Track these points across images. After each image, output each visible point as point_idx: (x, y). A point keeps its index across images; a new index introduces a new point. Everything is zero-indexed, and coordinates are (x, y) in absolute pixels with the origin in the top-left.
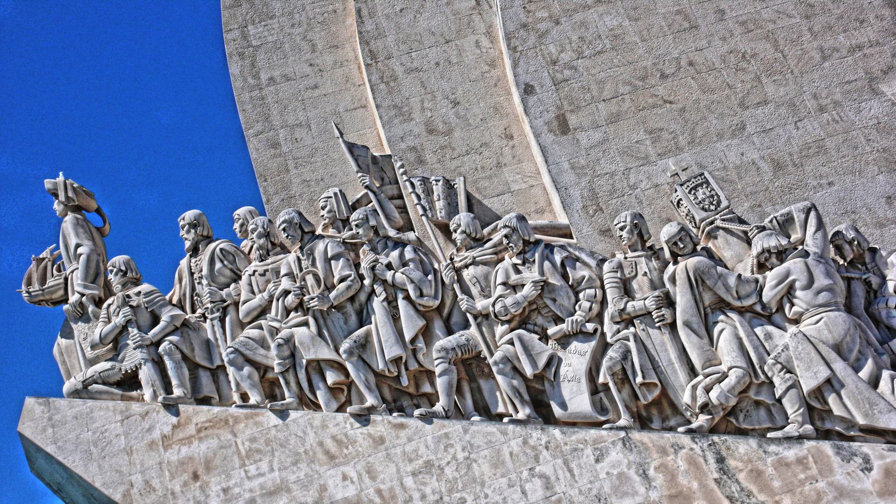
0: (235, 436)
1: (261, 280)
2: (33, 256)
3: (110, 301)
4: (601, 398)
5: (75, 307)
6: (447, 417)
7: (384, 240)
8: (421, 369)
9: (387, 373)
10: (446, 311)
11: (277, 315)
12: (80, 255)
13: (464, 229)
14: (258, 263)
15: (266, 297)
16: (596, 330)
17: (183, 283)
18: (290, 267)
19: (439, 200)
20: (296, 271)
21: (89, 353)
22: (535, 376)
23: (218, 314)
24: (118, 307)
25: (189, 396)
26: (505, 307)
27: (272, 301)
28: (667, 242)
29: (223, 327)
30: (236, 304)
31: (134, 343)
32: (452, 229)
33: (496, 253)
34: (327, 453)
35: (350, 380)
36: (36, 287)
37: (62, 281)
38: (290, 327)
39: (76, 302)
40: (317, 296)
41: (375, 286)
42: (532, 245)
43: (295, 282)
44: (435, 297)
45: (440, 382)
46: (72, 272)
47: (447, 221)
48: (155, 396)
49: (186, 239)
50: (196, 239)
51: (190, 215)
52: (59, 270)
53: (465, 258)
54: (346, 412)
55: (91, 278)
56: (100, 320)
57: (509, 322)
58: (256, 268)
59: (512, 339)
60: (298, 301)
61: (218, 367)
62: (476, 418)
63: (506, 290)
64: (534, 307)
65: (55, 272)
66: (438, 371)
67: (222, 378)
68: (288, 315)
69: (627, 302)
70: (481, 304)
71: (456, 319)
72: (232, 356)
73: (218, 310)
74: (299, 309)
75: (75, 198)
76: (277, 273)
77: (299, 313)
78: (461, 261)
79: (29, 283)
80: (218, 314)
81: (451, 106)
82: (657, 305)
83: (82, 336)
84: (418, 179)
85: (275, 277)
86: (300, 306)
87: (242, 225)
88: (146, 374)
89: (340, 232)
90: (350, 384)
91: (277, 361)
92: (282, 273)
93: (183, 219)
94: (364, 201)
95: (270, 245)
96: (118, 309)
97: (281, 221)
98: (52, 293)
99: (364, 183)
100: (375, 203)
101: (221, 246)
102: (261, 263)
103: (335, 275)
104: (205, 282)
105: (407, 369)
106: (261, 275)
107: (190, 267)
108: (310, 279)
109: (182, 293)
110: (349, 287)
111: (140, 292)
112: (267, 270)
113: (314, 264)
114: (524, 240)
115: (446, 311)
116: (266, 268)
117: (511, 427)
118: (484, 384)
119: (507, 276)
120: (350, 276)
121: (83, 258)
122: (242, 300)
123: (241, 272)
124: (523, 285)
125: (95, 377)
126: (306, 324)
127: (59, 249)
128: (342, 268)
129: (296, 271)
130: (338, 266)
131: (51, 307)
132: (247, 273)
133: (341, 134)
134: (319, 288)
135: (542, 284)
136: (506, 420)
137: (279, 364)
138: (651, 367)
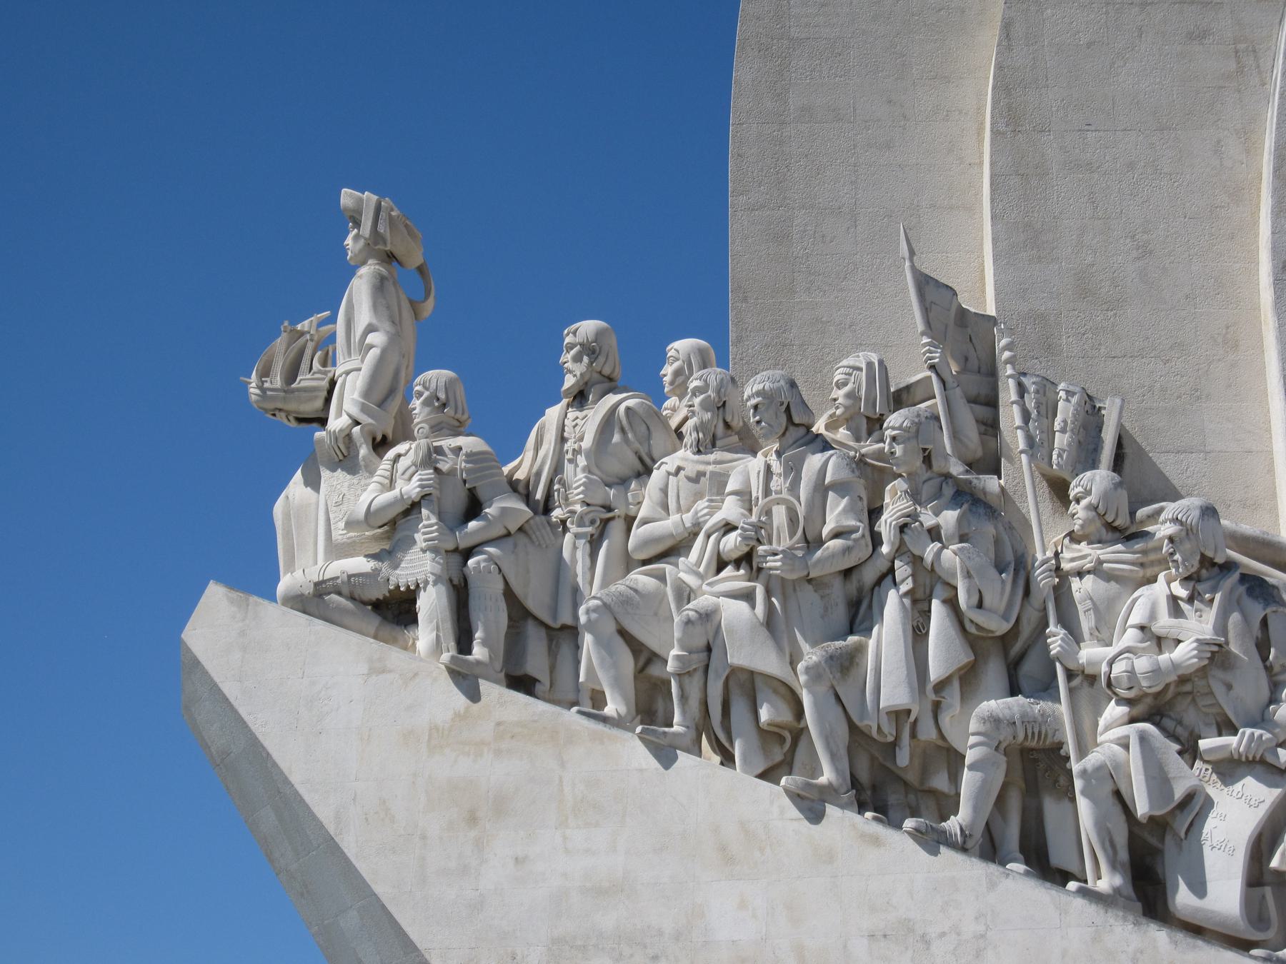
0: (563, 765)
1: (687, 487)
2: (286, 323)
3: (401, 448)
4: (1264, 897)
5: (336, 439)
6: (963, 849)
7: (939, 480)
8: (940, 743)
9: (874, 734)
10: (1016, 649)
12: (371, 347)
13: (1094, 502)
14: (689, 454)
15: (688, 524)
17: (541, 453)
18: (747, 482)
19: (1063, 431)
20: (757, 491)
21: (339, 533)
22: (1152, 819)
23: (589, 529)
24: (414, 464)
25: (498, 664)
26: (1132, 672)
27: (696, 535)
29: (593, 556)
30: (630, 521)
31: (426, 540)
32: (1072, 494)
33: (1142, 565)
34: (723, 848)
35: (802, 725)
36: (277, 381)
37: (325, 384)
38: (718, 595)
39: (341, 430)
40: (783, 552)
41: (897, 563)
42: (1216, 569)
43: (750, 511)
44: (1005, 617)
45: (969, 780)
46: (348, 373)
47: (1066, 476)
48: (437, 647)
49: (570, 371)
50: (586, 378)
51: (588, 327)
52: (324, 364)
54: (778, 783)
56: (375, 479)
59: (1128, 737)
60: (746, 549)
61: (564, 627)
62: (1018, 867)
63: (1142, 641)
64: (1188, 688)
65: (316, 365)
66: (970, 756)
67: (565, 650)
70: (1090, 653)
71: (1030, 667)
72: (594, 616)
73: (592, 522)
74: (744, 564)
75: (388, 236)
76: (719, 482)
77: (742, 572)
78: (1073, 560)
79: (265, 373)
80: (589, 529)
81: (1135, 254)
83: (335, 499)
84: (1035, 379)
85: (715, 490)
86: (746, 559)
87: (678, 373)
88: (431, 603)
89: (858, 440)
90: (800, 736)
91: (675, 652)
92: (729, 488)
93: (575, 333)
94: (919, 394)
95: (721, 425)
96: (413, 468)
97: (754, 391)
99: (930, 359)
100: (938, 400)
101: (631, 403)
102: (697, 457)
103: (827, 520)
104: (582, 461)
105: (913, 735)
106: (689, 479)
107: (564, 426)
108: (780, 514)
109: (534, 470)
110: (847, 550)
111: (460, 449)
112: (704, 474)
113: (794, 487)
114: (1203, 555)
115: (1016, 649)
116: (701, 468)
117: (1079, 902)
118: (1052, 809)
119: (1153, 615)
120: (856, 530)
121: (374, 354)
123: (654, 461)
124: (1179, 642)
125: (339, 581)
126: (748, 597)
127: (335, 322)
128: (845, 511)
129: (757, 491)
130: (838, 505)
131: (293, 424)
132: (664, 468)
133: (912, 253)
134: (791, 538)
135: (1215, 649)
136: (1072, 885)
137: (678, 657)
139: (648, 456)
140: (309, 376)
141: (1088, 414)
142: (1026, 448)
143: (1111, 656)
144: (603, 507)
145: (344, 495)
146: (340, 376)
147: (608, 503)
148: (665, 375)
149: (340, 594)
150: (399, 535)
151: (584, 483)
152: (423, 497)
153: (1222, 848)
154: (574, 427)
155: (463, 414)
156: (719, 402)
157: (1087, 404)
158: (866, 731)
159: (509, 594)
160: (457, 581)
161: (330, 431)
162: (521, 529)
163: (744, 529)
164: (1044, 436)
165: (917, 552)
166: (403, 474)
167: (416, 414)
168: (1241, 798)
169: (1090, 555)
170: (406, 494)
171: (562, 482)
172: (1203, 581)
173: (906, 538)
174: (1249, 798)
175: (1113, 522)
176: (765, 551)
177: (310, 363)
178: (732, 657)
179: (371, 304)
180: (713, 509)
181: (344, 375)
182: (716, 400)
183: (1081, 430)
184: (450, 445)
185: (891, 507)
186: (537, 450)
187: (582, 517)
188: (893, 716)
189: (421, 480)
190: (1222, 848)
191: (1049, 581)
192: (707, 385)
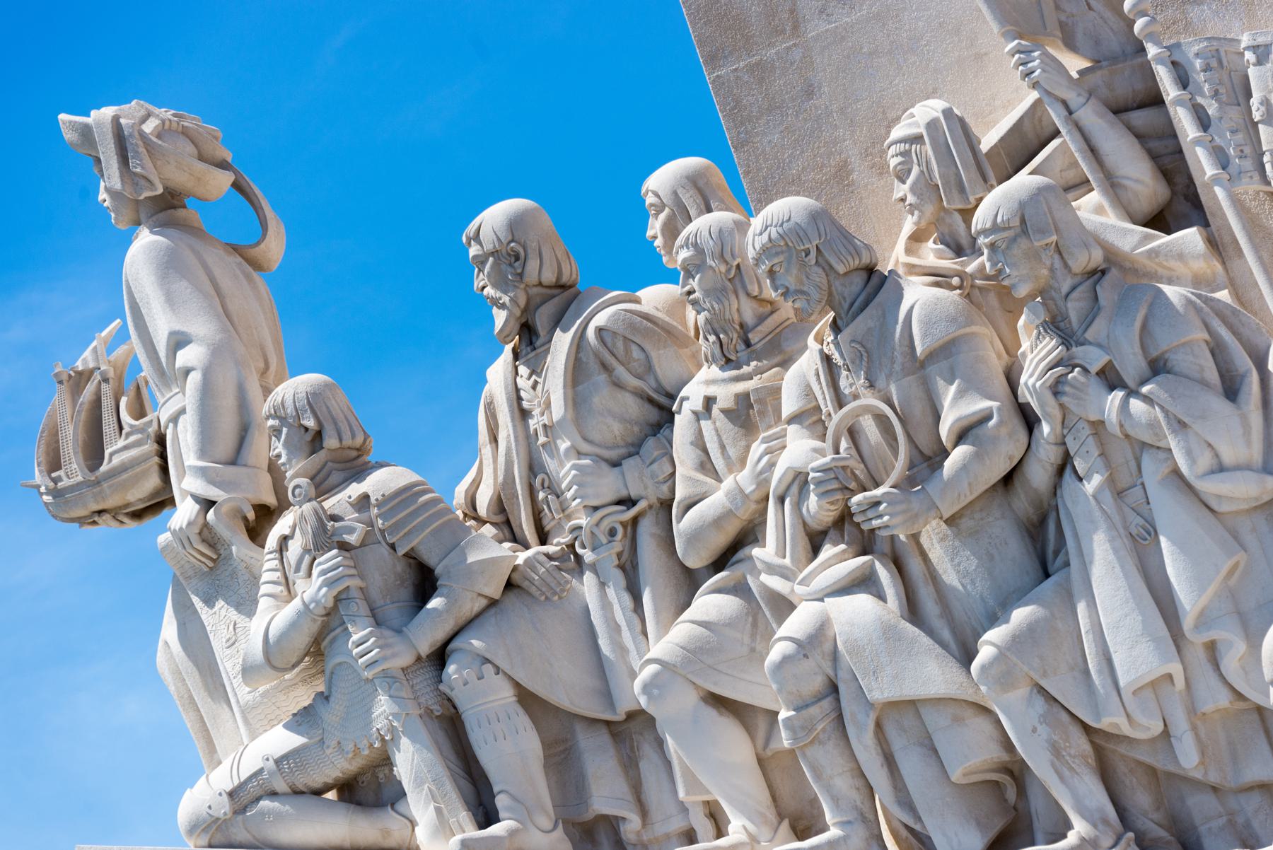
3: (282, 525)
12: (187, 372)
14: (714, 371)
20: (827, 404)
24: (306, 551)
30: (667, 505)
37: (150, 447)
39: (189, 524)
46: (175, 419)
48: (443, 827)
49: (495, 302)
50: (522, 301)
52: (140, 413)
55: (226, 444)
58: (712, 391)
68: (815, 550)
79: (54, 463)
90: (1016, 771)
96: (307, 559)
97: (758, 248)
98: (125, 486)
100: (1067, 140)
107: (517, 390)
109: (500, 479)
111: (365, 497)
121: (194, 379)
122: (680, 494)
123: (672, 397)
126: (864, 583)
128: (960, 394)
131: (132, 525)
139: (656, 391)
140: (121, 443)
142: (1216, 172)
144: (619, 502)
145: (235, 624)
146: (167, 427)
147: (624, 493)
148: (655, 237)
149: (273, 794)
150: (331, 663)
151: (575, 476)
152: (337, 599)
154: (534, 387)
155: (353, 436)
156: (729, 270)
158: (1117, 732)
159: (527, 699)
160: (439, 708)
161: (175, 530)
162: (510, 585)
163: (819, 483)
164: (1240, 137)
165: (1093, 417)
166: (297, 570)
167: (283, 464)
170: (311, 603)
171: (546, 484)
173: (1065, 399)
176: (859, 504)
177: (115, 419)
179: (163, 298)
180: (775, 451)
181: (171, 425)
182: (723, 268)
184: (350, 497)
185: (1030, 357)
186: (494, 439)
187: (592, 533)
188: (1148, 694)
189: (323, 573)
192: (699, 251)
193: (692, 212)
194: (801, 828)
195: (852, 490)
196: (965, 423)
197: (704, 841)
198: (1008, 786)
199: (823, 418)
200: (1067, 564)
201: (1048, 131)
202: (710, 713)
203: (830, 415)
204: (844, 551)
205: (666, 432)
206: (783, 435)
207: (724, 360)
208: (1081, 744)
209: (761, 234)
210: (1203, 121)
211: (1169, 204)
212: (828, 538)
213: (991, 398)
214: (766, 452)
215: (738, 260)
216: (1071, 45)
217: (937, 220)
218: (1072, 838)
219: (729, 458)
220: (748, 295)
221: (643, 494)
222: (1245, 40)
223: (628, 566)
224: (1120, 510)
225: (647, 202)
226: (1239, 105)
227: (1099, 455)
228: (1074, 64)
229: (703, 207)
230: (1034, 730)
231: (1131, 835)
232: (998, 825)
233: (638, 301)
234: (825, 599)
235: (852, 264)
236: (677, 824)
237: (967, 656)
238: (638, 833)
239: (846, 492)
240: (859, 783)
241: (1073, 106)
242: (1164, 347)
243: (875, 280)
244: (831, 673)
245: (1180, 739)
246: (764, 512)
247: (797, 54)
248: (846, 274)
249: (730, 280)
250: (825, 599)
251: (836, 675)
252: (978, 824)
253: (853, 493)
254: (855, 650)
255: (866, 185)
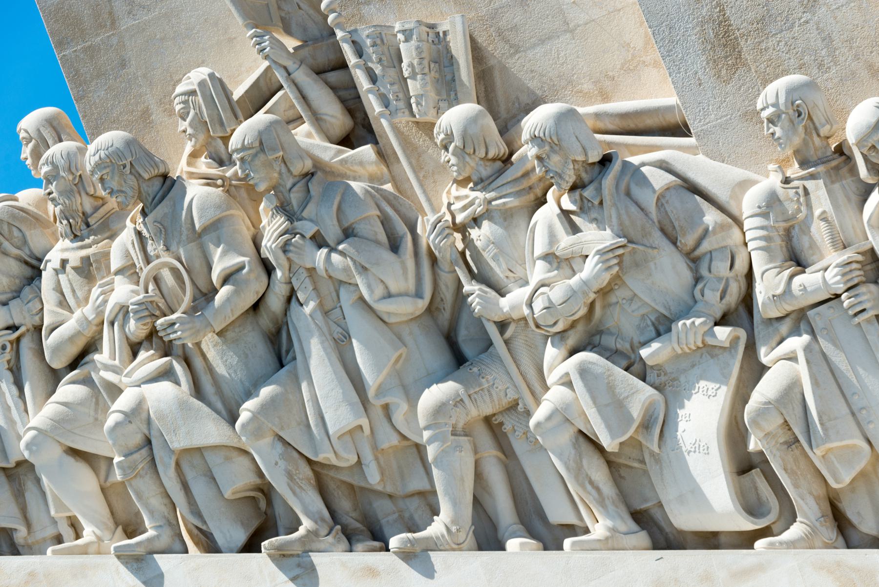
6: (458, 547)
10: (445, 316)
11: (113, 356)
14: (67, 243)
15: (91, 317)
16: (735, 340)
18: (127, 255)
19: (413, 76)
20: (139, 261)
27: (103, 323)
28: (859, 144)
30: (38, 329)
44: (419, 295)
53: (472, 203)
57: (562, 335)
58: (65, 256)
59: (567, 374)
61: (19, 464)
63: (549, 271)
67: (30, 486)
68: (135, 355)
69: (792, 277)
82: (845, 283)
90: (265, 490)
97: (92, 164)
100: (287, 91)
119: (552, 238)
122: (46, 322)
123: (40, 260)
126: (166, 374)
128: (224, 253)
138: (845, 410)
139: (30, 257)
141: (435, 44)
142: (381, 110)
143: (526, 297)
144: (8, 328)
147: (10, 322)
148: (26, 159)
153: (697, 449)
156: (74, 179)
157: (430, 34)
158: (328, 463)
163: (136, 312)
164: (396, 87)
165: (309, 266)
168: (698, 392)
169: (477, 198)
172: (587, 185)
173: (290, 255)
174: (705, 389)
175: (487, 153)
176: (162, 325)
178: (172, 443)
180: (108, 292)
182: (71, 177)
183: (432, 65)
185: (268, 228)
188: (348, 438)
190: (697, 449)
191: (445, 242)
192: (55, 166)
193: (50, 142)
194: (130, 531)
195: (157, 316)
196: (228, 271)
197: (67, 542)
198: (261, 499)
199: (137, 271)
200: (294, 358)
201: (275, 86)
202: (70, 461)
203: (141, 269)
204: (153, 355)
205: (36, 282)
206: (112, 282)
207: (73, 235)
208: (307, 471)
209: (94, 155)
210: (373, 78)
211: (353, 130)
212: (142, 348)
213: (244, 255)
214: (102, 293)
215: (80, 172)
216: (288, 32)
217: (207, 144)
218: (302, 531)
219: (78, 298)
220: (87, 194)
221: (23, 322)
222: (398, 27)
223: (14, 369)
224: (327, 324)
225: (21, 137)
226: (395, 67)
227: (313, 289)
228: (291, 43)
229: (56, 139)
230: (276, 464)
231: (339, 527)
232: (255, 524)
233: (16, 200)
234: (142, 386)
235: (153, 173)
236: (50, 532)
237: (232, 418)
238: (25, 538)
239: (153, 317)
240: (166, 501)
241: (290, 70)
242: (352, 221)
243: (168, 182)
244: (147, 432)
245: (368, 466)
246: (101, 332)
247: (114, 40)
248: (149, 179)
249: (75, 185)
250: (142, 386)
251: (150, 433)
252: (242, 524)
253: (158, 318)
254: (162, 417)
255: (161, 123)
